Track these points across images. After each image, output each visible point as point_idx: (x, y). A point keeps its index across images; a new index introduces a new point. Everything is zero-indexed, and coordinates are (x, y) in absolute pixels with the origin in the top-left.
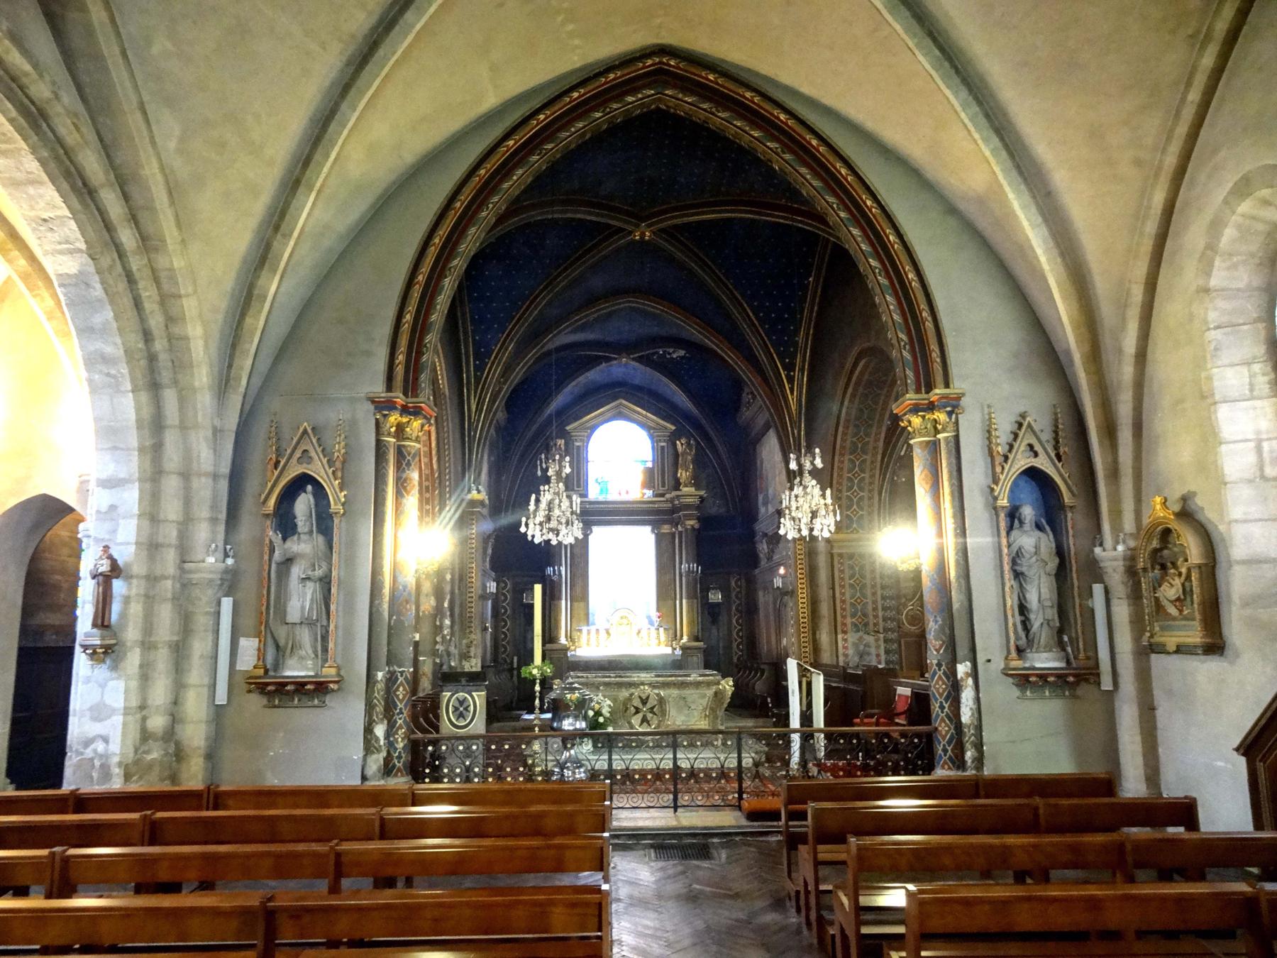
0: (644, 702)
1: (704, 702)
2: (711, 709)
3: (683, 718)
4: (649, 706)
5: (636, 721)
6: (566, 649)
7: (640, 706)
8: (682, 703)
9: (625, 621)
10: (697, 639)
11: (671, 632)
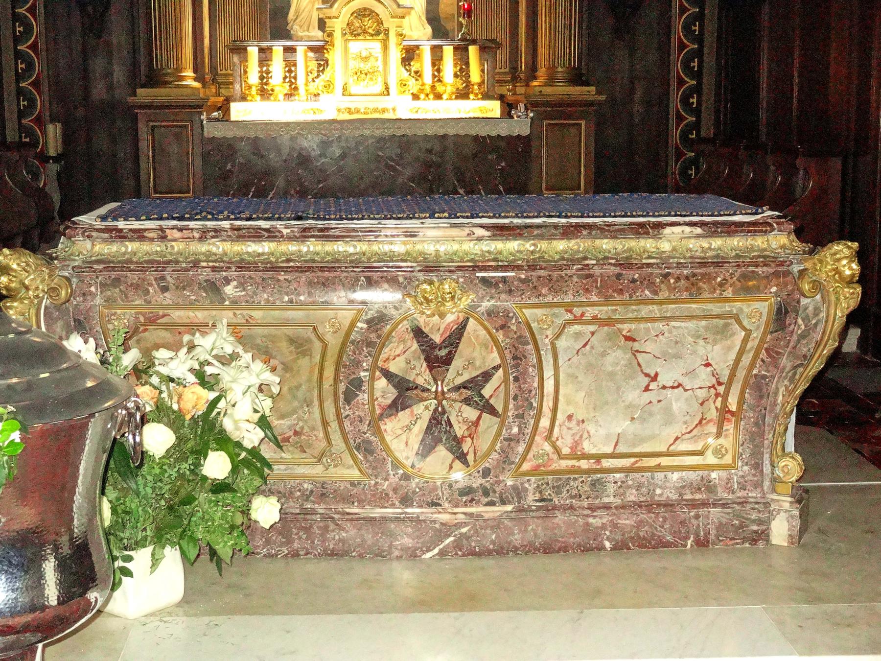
0: (438, 355)
1: (722, 356)
2: (758, 387)
3: (622, 426)
4: (458, 372)
5: (403, 436)
6: (196, 106)
7: (421, 375)
8: (617, 358)
9: (369, 23)
10: (577, 78)
11: (503, 55)
